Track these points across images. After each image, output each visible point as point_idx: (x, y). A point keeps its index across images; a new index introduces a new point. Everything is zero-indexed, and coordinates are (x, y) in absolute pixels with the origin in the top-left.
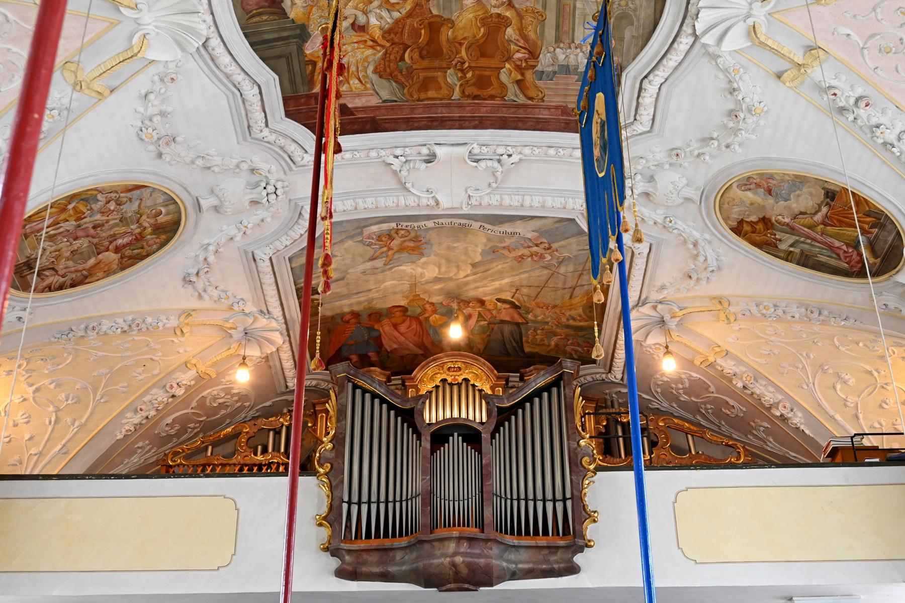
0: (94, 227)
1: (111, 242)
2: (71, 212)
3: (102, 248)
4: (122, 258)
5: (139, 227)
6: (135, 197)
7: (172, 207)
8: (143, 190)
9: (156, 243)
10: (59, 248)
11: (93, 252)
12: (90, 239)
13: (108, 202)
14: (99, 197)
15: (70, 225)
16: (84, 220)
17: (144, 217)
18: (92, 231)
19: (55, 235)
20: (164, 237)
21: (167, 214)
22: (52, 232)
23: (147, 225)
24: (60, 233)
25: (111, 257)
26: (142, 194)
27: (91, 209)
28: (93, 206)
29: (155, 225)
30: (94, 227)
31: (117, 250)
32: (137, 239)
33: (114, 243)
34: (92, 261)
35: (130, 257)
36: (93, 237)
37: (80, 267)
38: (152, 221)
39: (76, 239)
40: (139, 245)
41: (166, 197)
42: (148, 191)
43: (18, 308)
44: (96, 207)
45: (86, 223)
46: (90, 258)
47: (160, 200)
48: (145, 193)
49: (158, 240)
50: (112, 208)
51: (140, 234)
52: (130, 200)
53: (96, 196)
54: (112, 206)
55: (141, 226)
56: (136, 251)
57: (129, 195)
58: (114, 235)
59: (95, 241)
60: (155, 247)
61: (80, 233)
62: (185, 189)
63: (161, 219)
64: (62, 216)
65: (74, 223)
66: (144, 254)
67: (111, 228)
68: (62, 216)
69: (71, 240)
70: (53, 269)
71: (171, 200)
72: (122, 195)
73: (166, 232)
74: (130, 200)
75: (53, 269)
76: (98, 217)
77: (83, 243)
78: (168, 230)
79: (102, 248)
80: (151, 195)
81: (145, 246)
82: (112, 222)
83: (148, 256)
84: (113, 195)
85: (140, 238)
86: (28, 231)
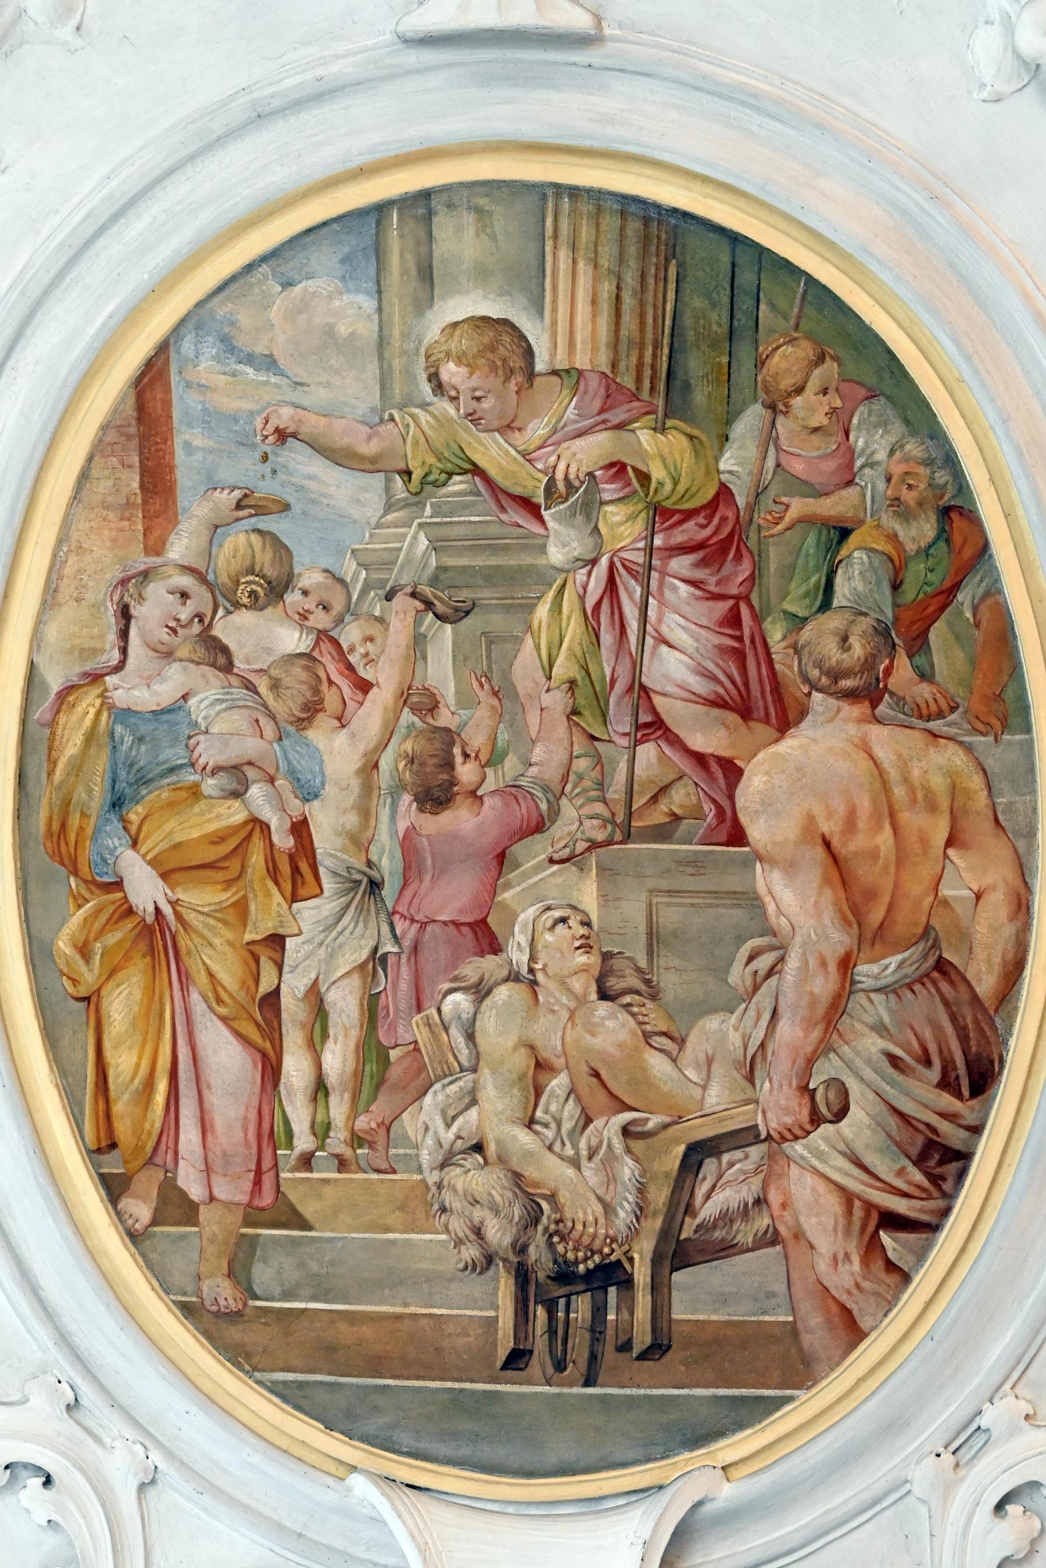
0: (436, 795)
1: (654, 728)
2: (202, 898)
3: (680, 798)
4: (869, 693)
5: (590, 508)
6: (243, 470)
7: (457, 239)
8: (184, 403)
9: (841, 424)
10: (521, 1061)
11: (695, 864)
12: (533, 853)
13: (218, 656)
14: (139, 690)
15: (324, 946)
16: (326, 841)
17: (492, 452)
18: (460, 819)
19: (372, 1051)
20: (786, 360)
21: (533, 282)
22: (337, 1059)
23: (588, 452)
24: (372, 1010)
25: (802, 774)
26: (210, 417)
27: (237, 777)
28: (208, 753)
29: (612, 394)
30: (436, 795)
31: (761, 701)
32: (715, 552)
33: (674, 711)
34: (795, 900)
35: (909, 629)
36: (539, 827)
37: (803, 981)
38: (553, 410)
39: (486, 939)
40: (783, 554)
41: (324, 259)
42: (201, 366)
43: (924, 1475)
44: (224, 727)
45: (359, 841)
46: (753, 902)
47: (353, 311)
48: (205, 385)
49: (811, 407)
50: (292, 640)
51: (661, 515)
52: (247, 503)
53: (125, 715)
54: (266, 637)
55: (581, 497)
56: (847, 587)
57: (196, 509)
58: (585, 700)
59: (574, 821)
60: (875, 441)
61: (450, 897)
62: (261, 117)
63: (572, 325)
64: (217, 958)
65: (312, 913)
66: (927, 528)
67: (503, 693)
68: (217, 958)
69: (474, 968)
70: (698, 1153)
71: (389, 233)
72: (180, 547)
73: (739, 331)
74: (247, 503)
75: (698, 1153)
76: (336, 752)
77: (547, 908)
78: (707, 307)
79: (680, 798)
80: (270, 363)
81: (832, 506)
82: (441, 671)
83: (955, 513)
84: (154, 608)
85: (716, 534)
86: (232, 1190)
